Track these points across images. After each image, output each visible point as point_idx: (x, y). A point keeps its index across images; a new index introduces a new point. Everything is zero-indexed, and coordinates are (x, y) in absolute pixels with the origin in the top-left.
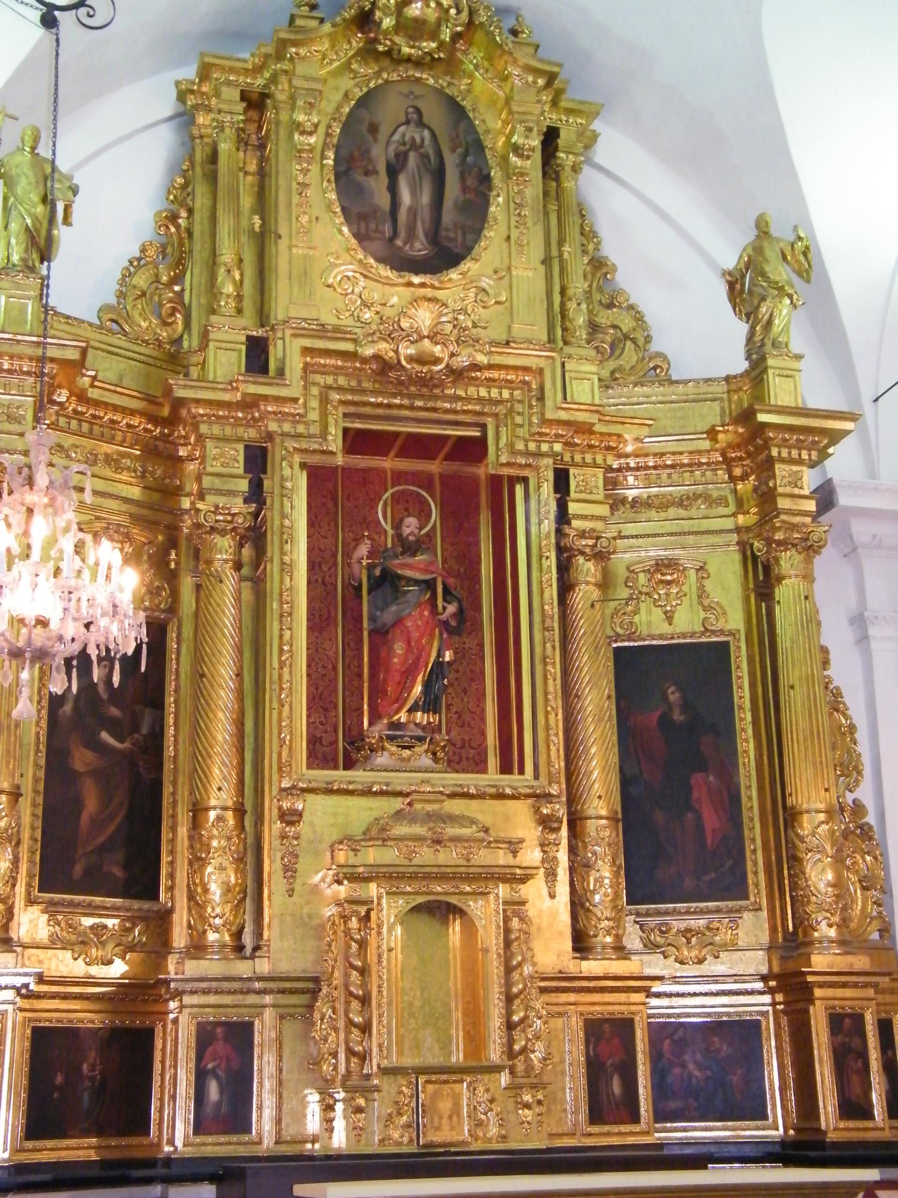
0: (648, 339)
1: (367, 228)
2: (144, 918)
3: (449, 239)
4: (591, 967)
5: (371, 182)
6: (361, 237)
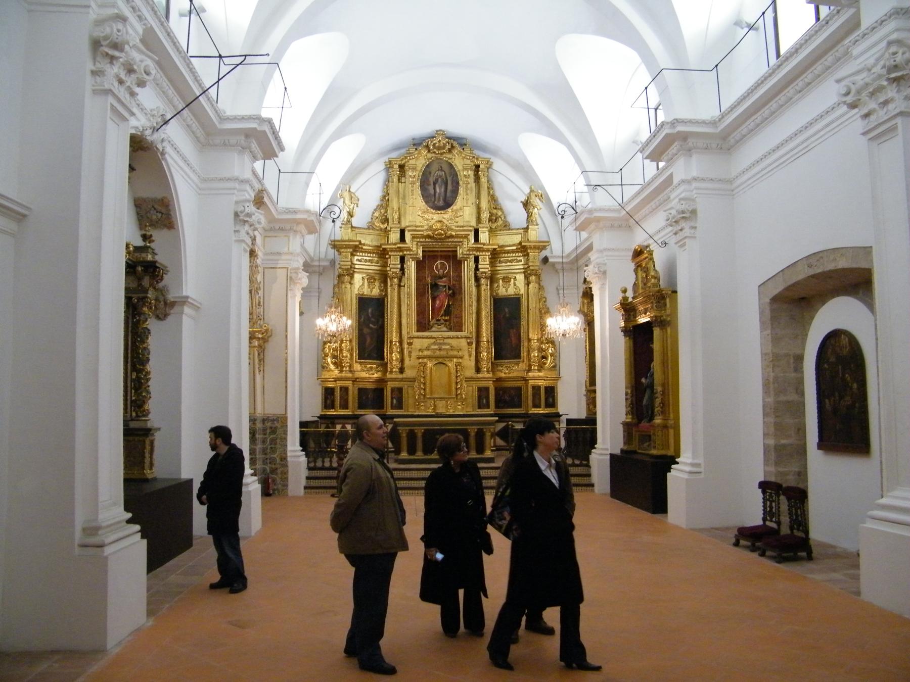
2: (382, 365)
4: (480, 375)
6: (426, 202)
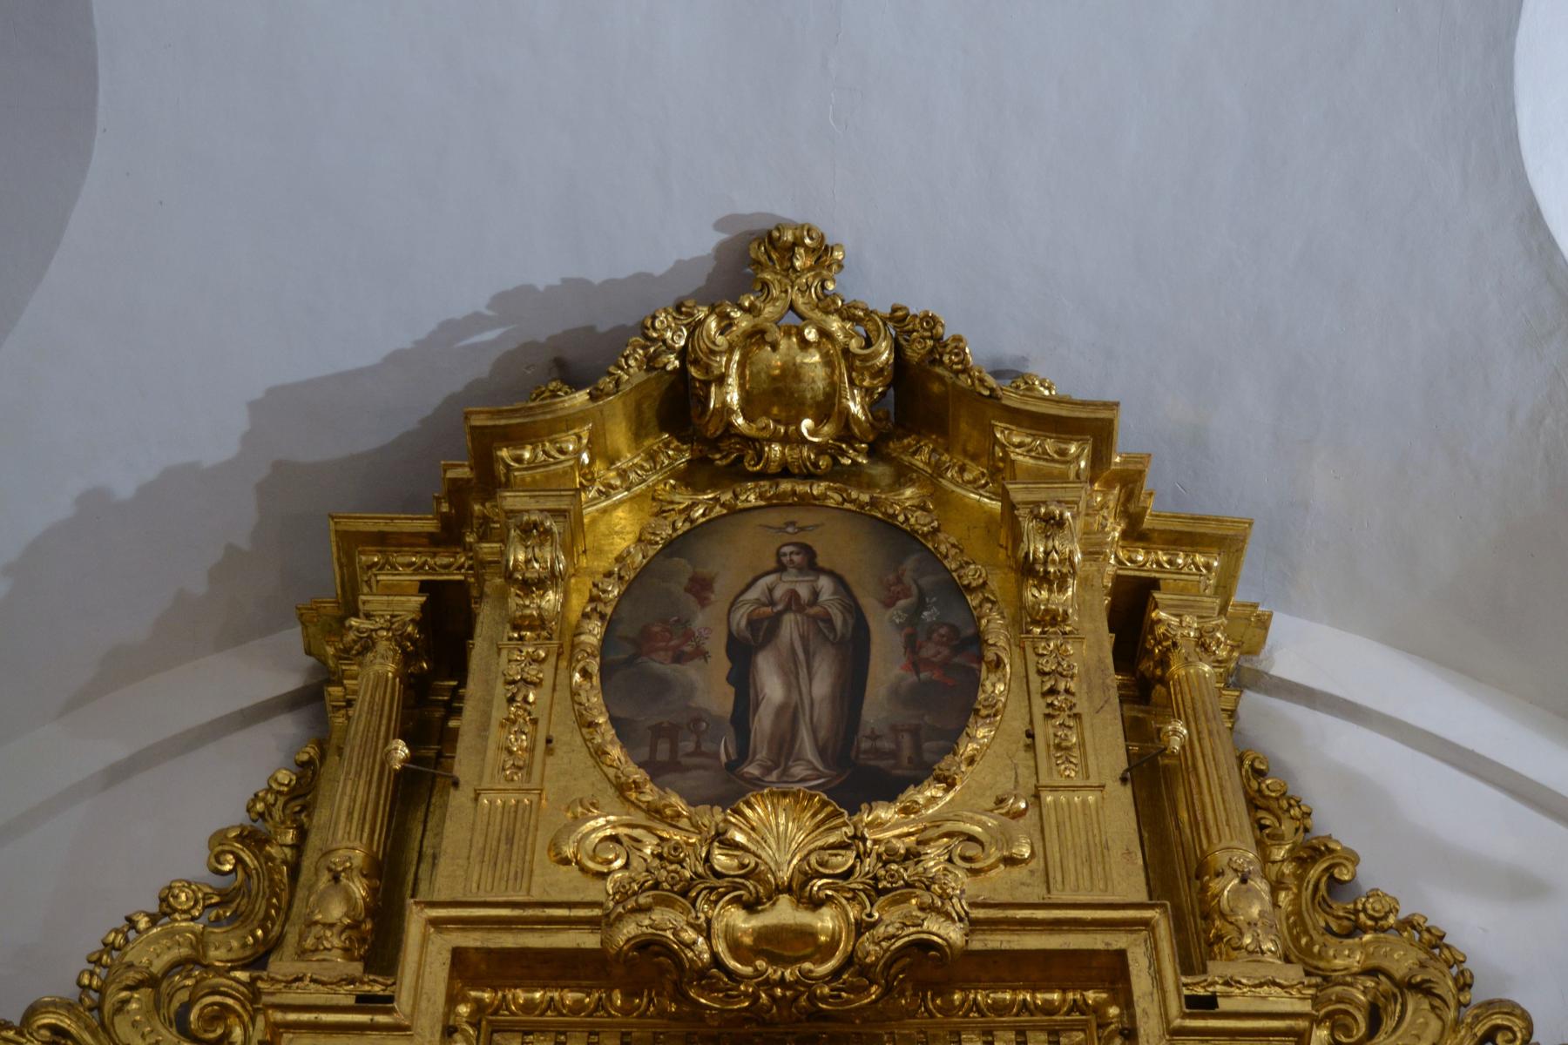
0: (1464, 985)
1: (674, 750)
3: (878, 753)
5: (691, 672)
